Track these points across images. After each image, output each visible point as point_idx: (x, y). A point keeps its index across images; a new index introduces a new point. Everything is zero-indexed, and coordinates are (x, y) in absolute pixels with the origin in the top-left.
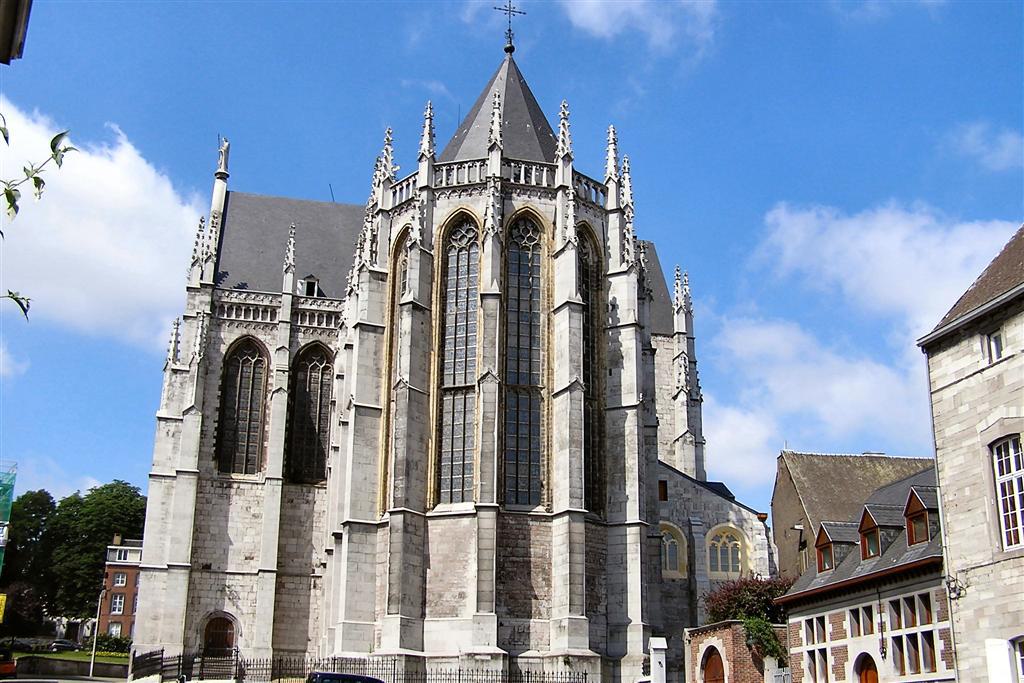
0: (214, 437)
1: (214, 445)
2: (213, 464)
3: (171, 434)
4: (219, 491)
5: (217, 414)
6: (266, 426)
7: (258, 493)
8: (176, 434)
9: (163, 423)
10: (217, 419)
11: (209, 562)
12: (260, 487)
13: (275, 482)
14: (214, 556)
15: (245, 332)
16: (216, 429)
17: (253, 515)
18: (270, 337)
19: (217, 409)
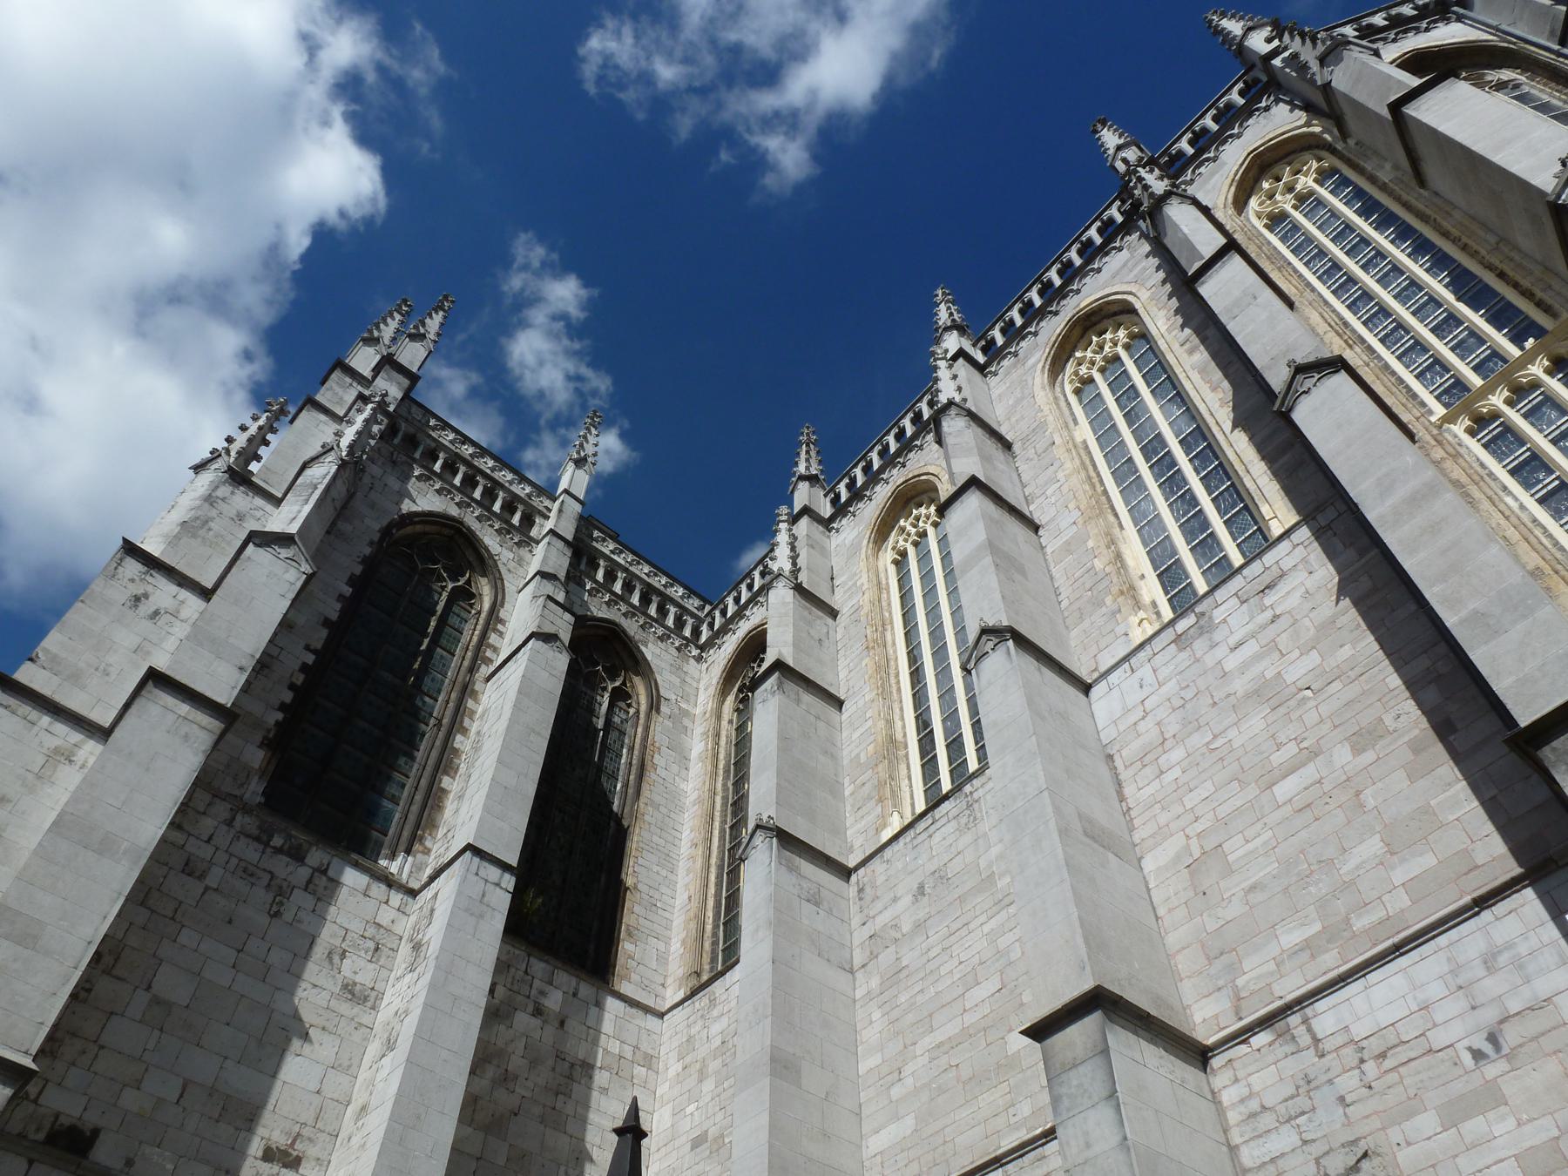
0: (292, 687)
1: (283, 707)
2: (256, 757)
3: (146, 608)
4: (251, 852)
5: (324, 633)
6: (459, 738)
7: (386, 916)
8: (165, 618)
9: (133, 567)
10: (318, 645)
11: (92, 1119)
12: (396, 898)
13: (493, 873)
14: (130, 1099)
15: (454, 511)
16: (304, 668)
17: (345, 987)
18: (511, 556)
19: (327, 623)
